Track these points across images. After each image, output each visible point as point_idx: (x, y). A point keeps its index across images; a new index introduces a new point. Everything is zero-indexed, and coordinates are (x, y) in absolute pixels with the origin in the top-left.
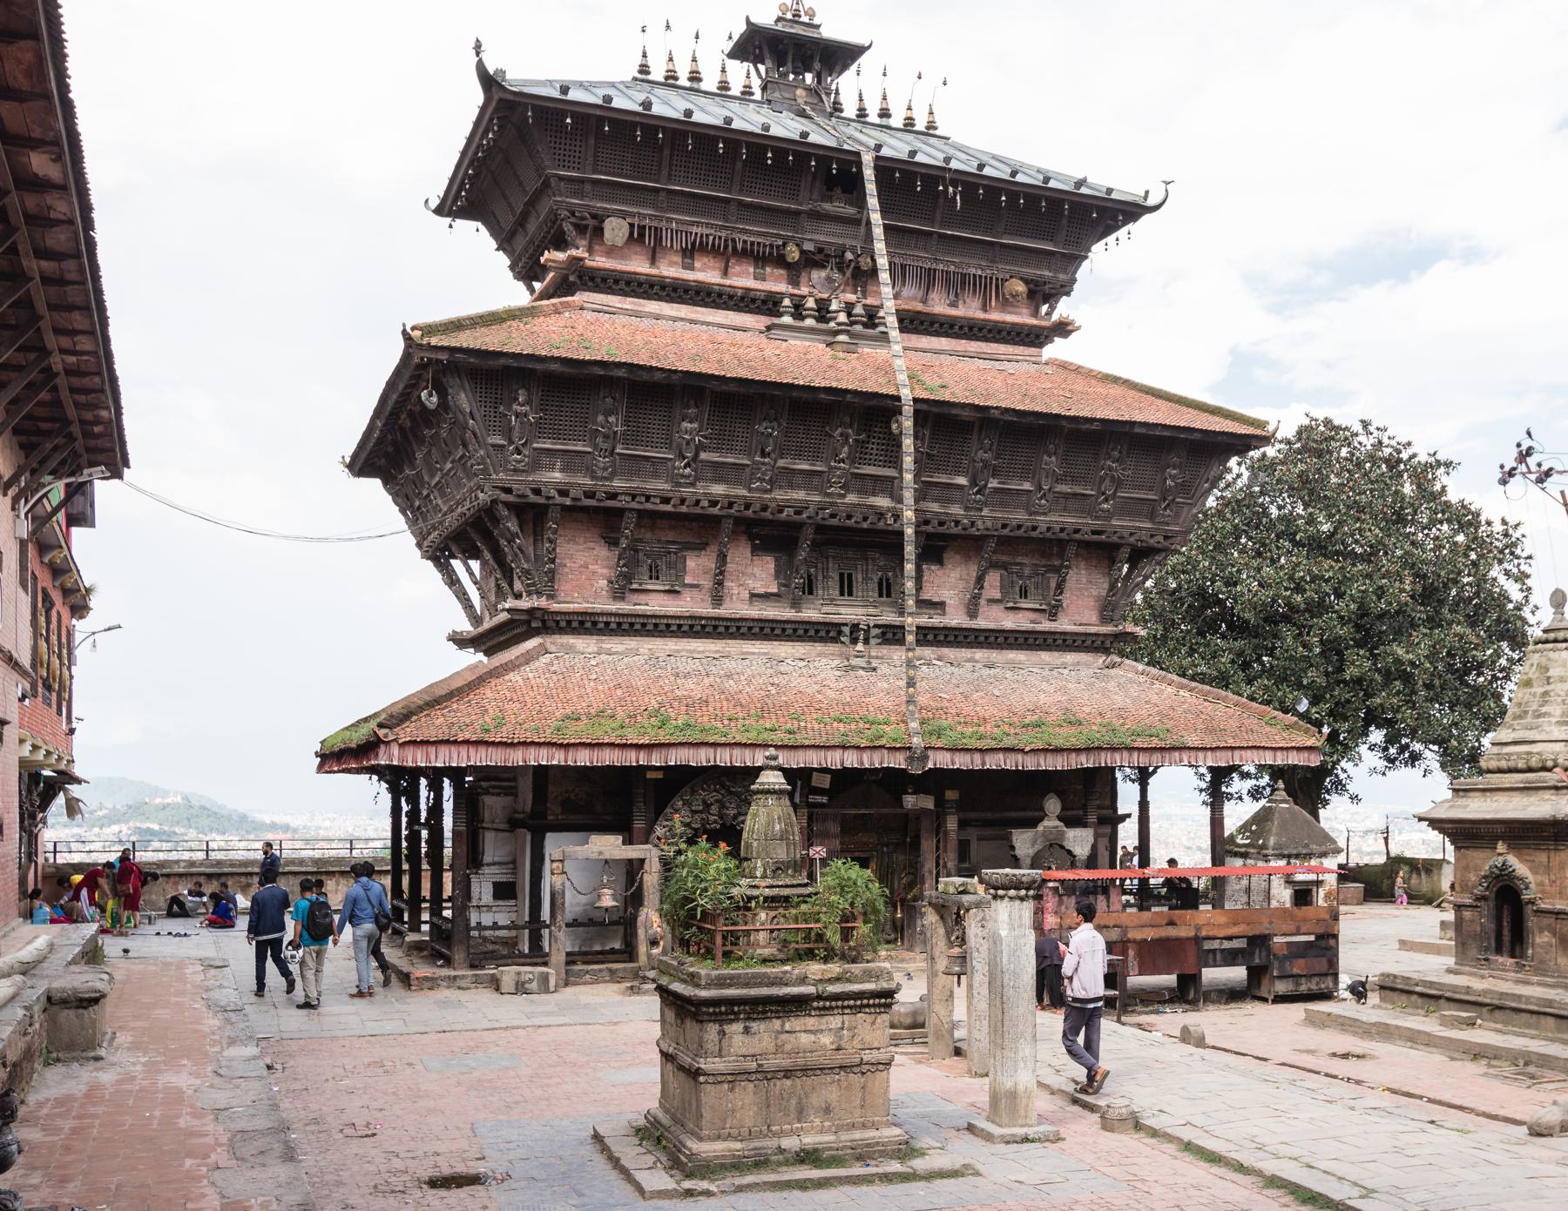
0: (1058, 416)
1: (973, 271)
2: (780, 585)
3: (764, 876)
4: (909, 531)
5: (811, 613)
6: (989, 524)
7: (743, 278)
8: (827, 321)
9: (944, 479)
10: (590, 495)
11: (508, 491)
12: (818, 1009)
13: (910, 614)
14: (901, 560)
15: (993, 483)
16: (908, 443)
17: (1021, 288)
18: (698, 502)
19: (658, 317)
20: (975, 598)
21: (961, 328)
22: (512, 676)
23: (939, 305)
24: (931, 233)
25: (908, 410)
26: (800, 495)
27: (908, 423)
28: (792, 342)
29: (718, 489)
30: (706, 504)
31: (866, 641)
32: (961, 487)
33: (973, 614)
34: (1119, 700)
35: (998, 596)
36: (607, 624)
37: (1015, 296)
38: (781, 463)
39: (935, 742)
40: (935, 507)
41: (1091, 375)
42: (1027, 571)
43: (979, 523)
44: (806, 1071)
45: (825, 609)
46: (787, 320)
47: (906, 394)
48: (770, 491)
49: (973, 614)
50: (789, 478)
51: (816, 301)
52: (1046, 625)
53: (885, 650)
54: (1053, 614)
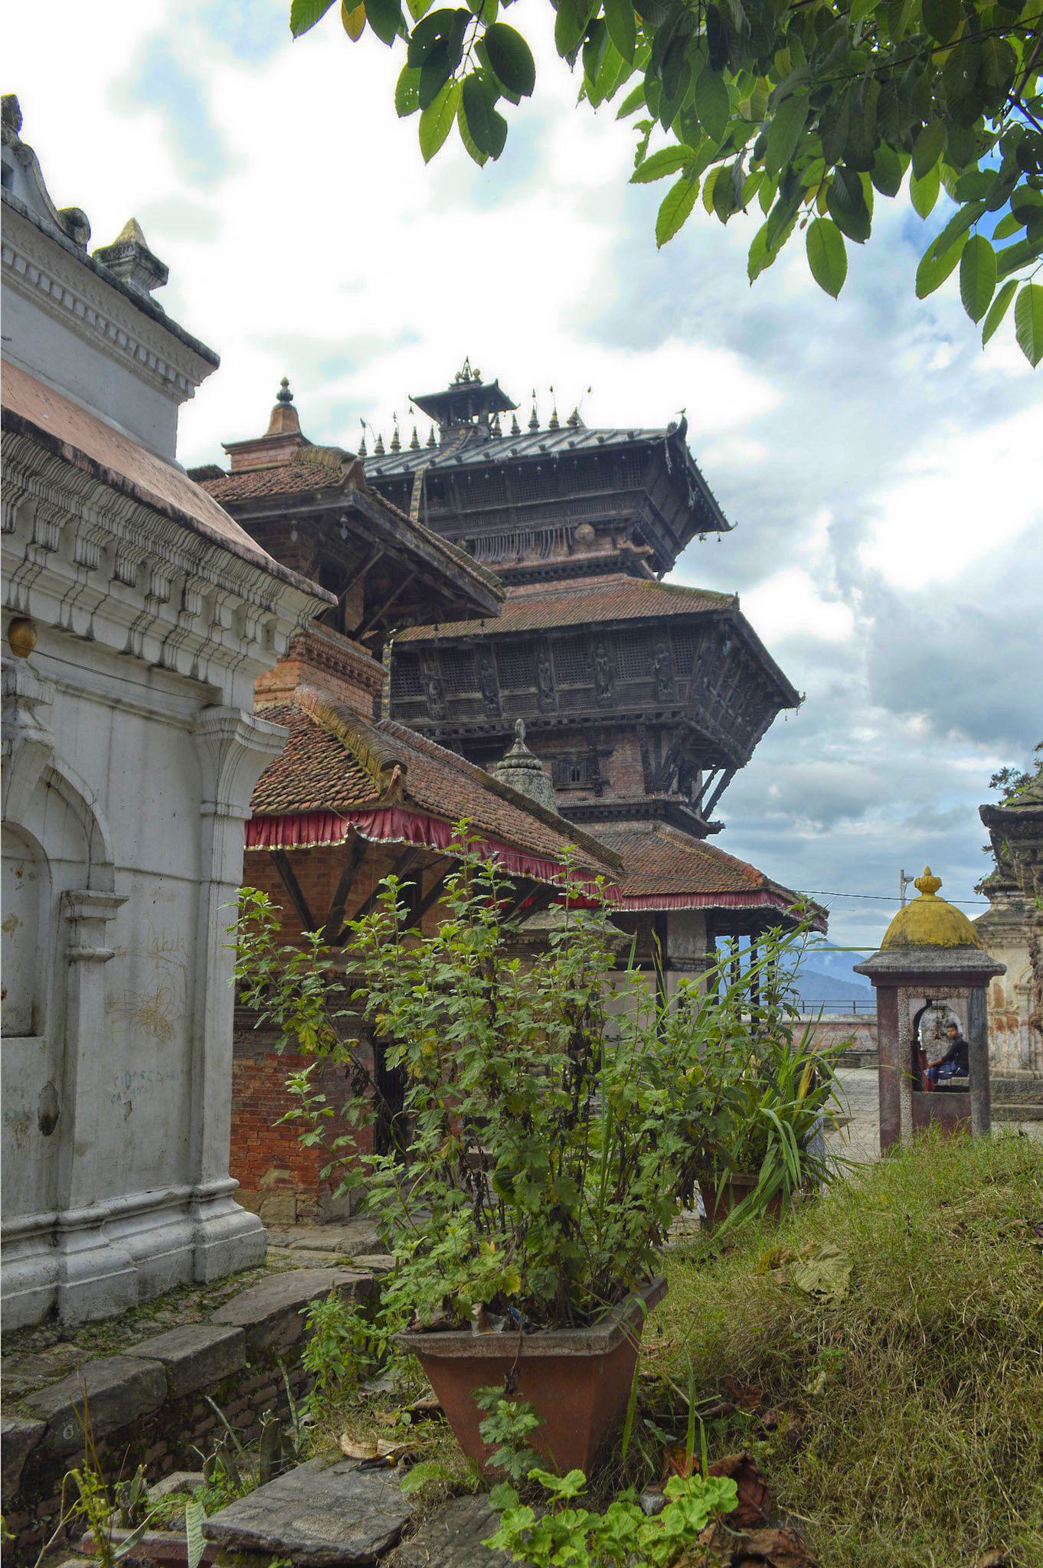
1: (544, 528)
9: (463, 696)
17: (586, 530)
21: (547, 573)
23: (532, 560)
24: (507, 509)
32: (479, 700)
40: (465, 719)
42: (574, 758)
43: (498, 728)
52: (592, 801)
54: (599, 793)
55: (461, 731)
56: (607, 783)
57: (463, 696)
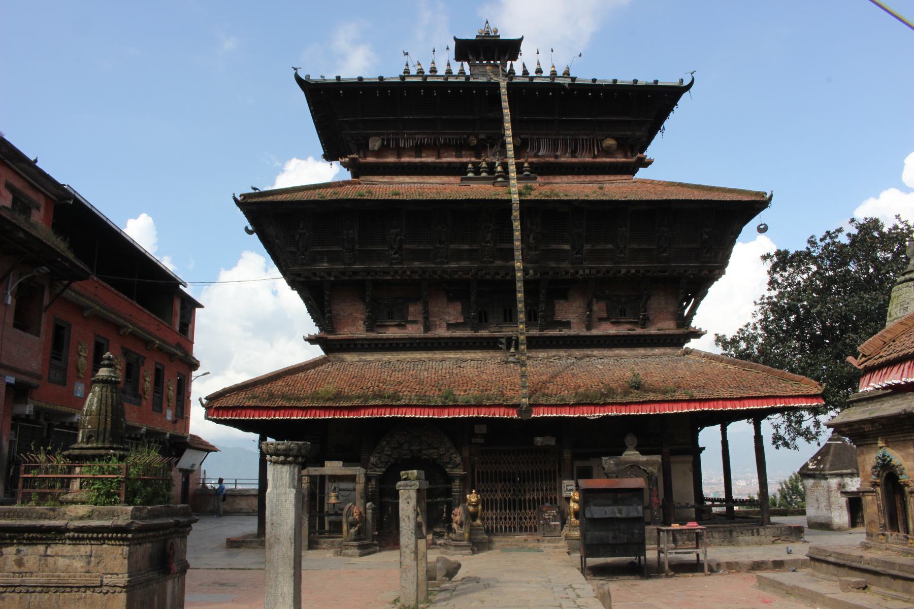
0: (617, 202)
1: (581, 137)
2: (465, 318)
3: (82, 441)
4: (519, 274)
5: (484, 333)
6: (587, 271)
7: (449, 159)
8: (495, 172)
9: (555, 246)
10: (343, 273)
11: (299, 275)
12: (69, 538)
13: (522, 323)
14: (514, 292)
15: (587, 247)
16: (517, 224)
18: (405, 272)
19: (402, 183)
20: (589, 316)
22: (302, 375)
25: (516, 205)
26: (465, 264)
27: (516, 214)
28: (472, 186)
29: (417, 264)
30: (409, 273)
31: (517, 348)
32: (567, 251)
33: (589, 328)
34: (681, 373)
35: (605, 315)
36: (363, 345)
37: (609, 147)
38: (452, 246)
39: (542, 401)
40: (553, 264)
41: (660, 183)
43: (581, 272)
44: (61, 587)
45: (493, 329)
46: (470, 175)
47: (515, 197)
48: (448, 263)
49: (589, 328)
50: (459, 256)
51: (487, 163)
52: (639, 331)
53: (533, 354)
55: (551, 273)
56: (648, 319)
57: (555, 246)
